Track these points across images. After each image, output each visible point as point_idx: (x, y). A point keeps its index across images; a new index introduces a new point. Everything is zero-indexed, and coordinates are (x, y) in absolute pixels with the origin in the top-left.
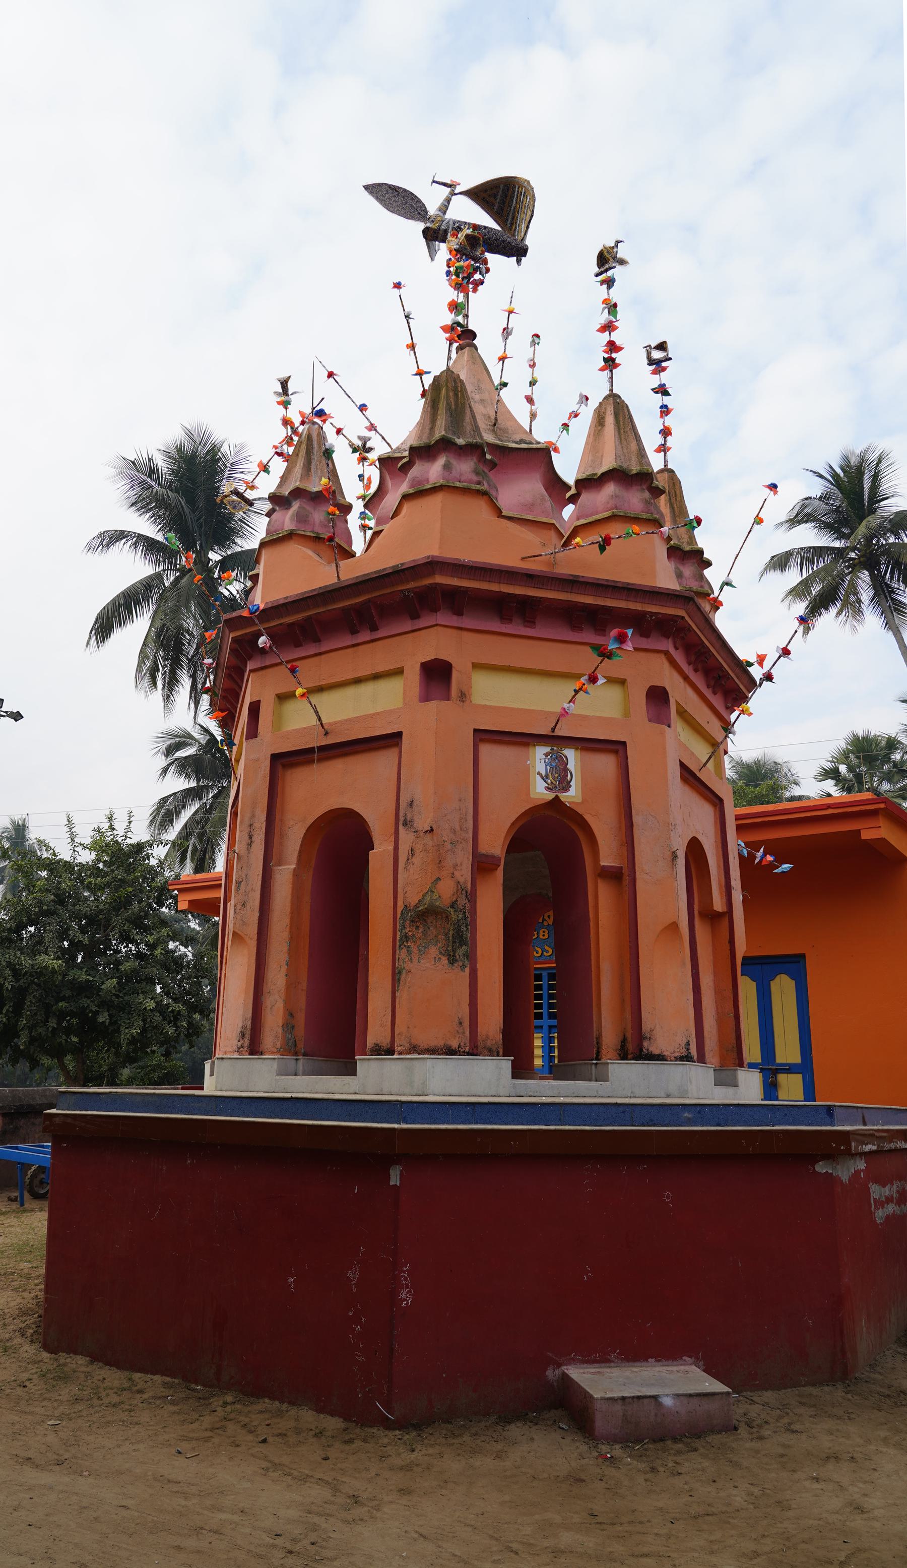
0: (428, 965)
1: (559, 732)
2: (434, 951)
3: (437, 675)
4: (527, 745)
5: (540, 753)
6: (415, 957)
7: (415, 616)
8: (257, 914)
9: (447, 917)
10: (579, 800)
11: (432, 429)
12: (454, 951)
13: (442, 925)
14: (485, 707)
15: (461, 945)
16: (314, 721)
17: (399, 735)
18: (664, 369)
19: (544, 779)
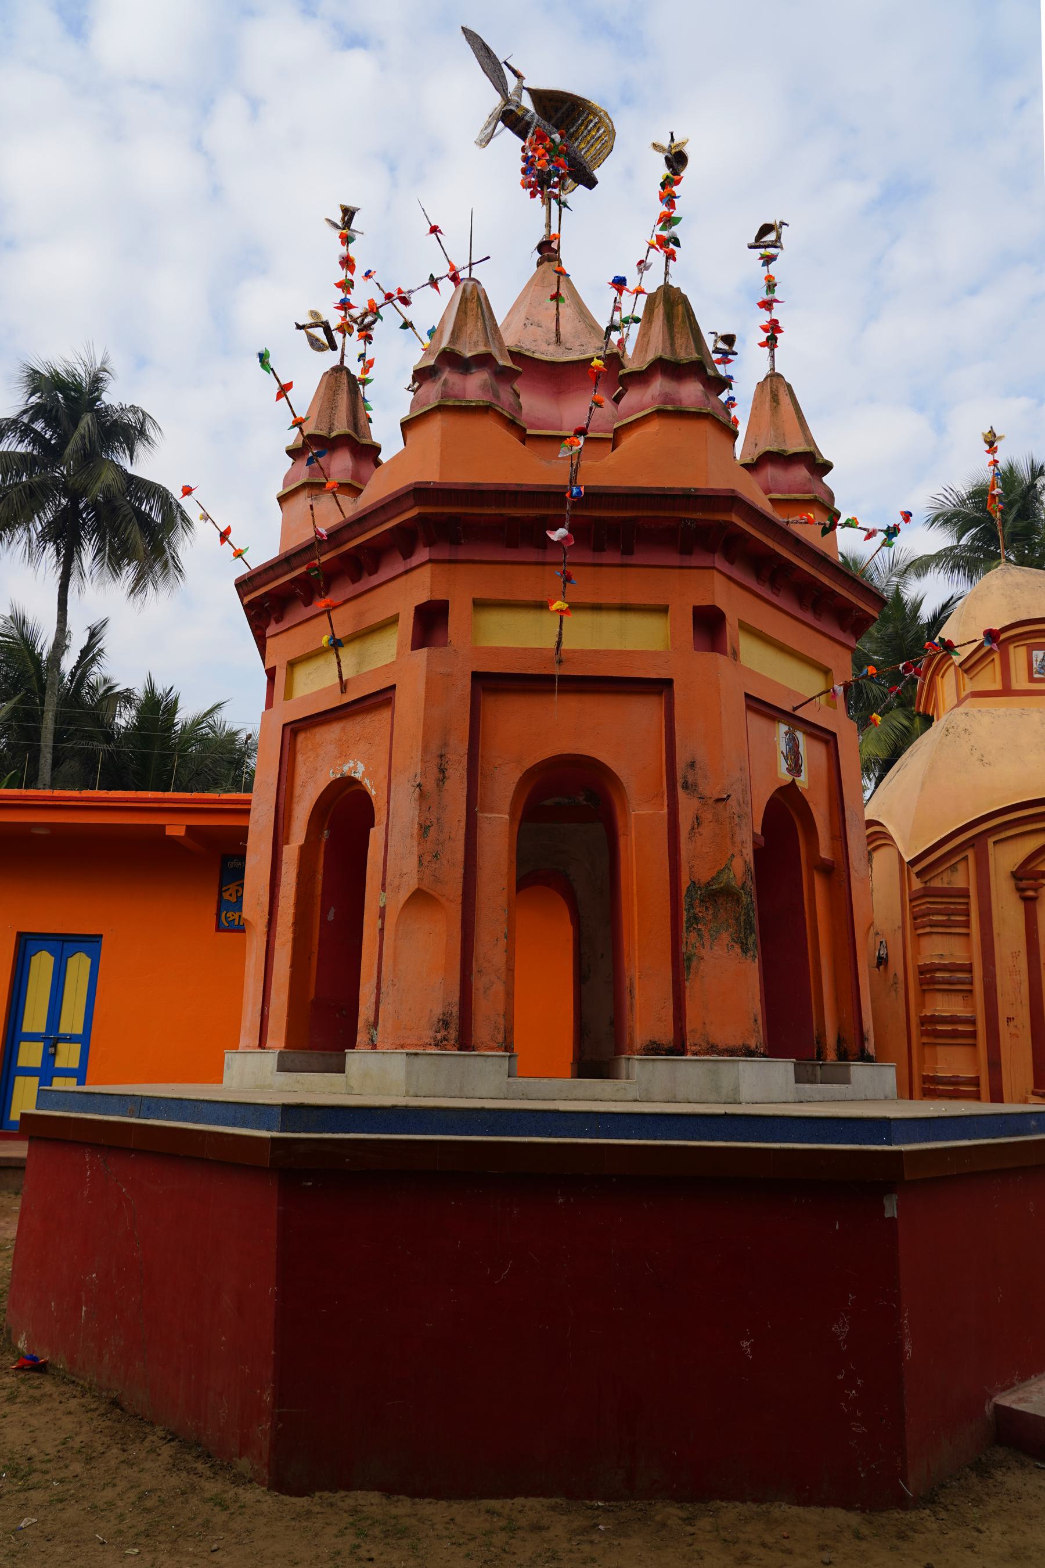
0: (720, 952)
1: (799, 713)
2: (725, 937)
3: (709, 626)
4: (773, 719)
5: (783, 728)
6: (707, 944)
7: (686, 550)
8: (460, 871)
9: (738, 900)
10: (806, 786)
11: (672, 344)
12: (746, 938)
13: (691, 904)
14: (750, 671)
15: (751, 933)
16: (552, 645)
17: (668, 683)
18: (730, 361)
19: (786, 759)
